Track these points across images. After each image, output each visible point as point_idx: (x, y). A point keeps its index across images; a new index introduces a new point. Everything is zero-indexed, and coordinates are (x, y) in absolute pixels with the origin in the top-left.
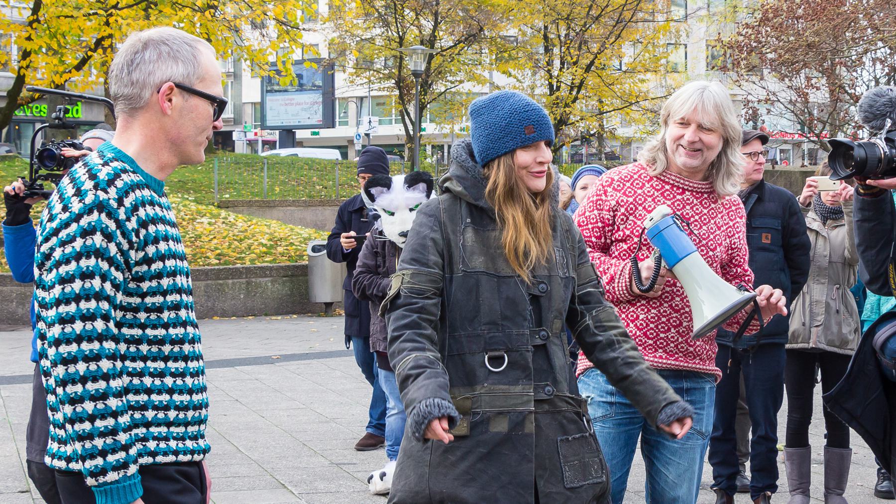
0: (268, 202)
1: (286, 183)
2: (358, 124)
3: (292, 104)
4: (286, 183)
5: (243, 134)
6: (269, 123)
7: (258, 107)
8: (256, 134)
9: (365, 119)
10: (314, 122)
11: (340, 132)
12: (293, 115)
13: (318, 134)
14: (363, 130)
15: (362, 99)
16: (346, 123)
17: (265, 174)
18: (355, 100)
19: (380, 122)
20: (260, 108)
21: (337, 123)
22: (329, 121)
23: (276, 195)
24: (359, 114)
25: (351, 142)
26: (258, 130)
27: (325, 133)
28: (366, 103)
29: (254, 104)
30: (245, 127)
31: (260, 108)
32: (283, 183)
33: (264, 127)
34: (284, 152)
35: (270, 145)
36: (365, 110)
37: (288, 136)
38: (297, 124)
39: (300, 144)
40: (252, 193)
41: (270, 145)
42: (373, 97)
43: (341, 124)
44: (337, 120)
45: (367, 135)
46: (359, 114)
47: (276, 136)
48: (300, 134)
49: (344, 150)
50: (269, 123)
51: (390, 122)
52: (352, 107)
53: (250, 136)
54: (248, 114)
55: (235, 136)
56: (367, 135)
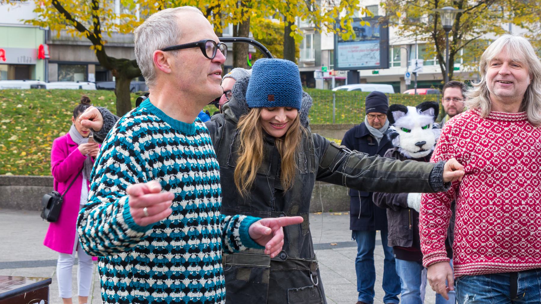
0: (336, 126)
1: (351, 111)
2: (408, 64)
3: (357, 51)
4: (351, 111)
5: (320, 74)
6: (340, 65)
7: (333, 52)
8: (330, 73)
9: (413, 61)
11: (393, 71)
12: (358, 59)
13: (377, 73)
14: (411, 69)
15: (410, 46)
16: (399, 65)
17: (334, 104)
18: (405, 47)
19: (425, 64)
20: (334, 53)
21: (392, 65)
22: (385, 63)
23: (342, 120)
24: (409, 57)
25: (402, 78)
26: (332, 71)
27: (383, 72)
28: (413, 48)
29: (330, 51)
30: (323, 69)
31: (334, 53)
32: (349, 111)
33: (336, 68)
34: (350, 87)
35: (340, 82)
36: (413, 54)
37: (354, 75)
38: (361, 66)
39: (364, 81)
40: (325, 120)
41: (340, 82)
42: (420, 45)
43: (395, 65)
44: (392, 62)
45: (415, 74)
46: (409, 57)
47: (344, 75)
48: (363, 73)
49: (396, 85)
50: (340, 65)
51: (432, 63)
53: (327, 75)
54: (326, 58)
55: (316, 75)
56: (415, 74)
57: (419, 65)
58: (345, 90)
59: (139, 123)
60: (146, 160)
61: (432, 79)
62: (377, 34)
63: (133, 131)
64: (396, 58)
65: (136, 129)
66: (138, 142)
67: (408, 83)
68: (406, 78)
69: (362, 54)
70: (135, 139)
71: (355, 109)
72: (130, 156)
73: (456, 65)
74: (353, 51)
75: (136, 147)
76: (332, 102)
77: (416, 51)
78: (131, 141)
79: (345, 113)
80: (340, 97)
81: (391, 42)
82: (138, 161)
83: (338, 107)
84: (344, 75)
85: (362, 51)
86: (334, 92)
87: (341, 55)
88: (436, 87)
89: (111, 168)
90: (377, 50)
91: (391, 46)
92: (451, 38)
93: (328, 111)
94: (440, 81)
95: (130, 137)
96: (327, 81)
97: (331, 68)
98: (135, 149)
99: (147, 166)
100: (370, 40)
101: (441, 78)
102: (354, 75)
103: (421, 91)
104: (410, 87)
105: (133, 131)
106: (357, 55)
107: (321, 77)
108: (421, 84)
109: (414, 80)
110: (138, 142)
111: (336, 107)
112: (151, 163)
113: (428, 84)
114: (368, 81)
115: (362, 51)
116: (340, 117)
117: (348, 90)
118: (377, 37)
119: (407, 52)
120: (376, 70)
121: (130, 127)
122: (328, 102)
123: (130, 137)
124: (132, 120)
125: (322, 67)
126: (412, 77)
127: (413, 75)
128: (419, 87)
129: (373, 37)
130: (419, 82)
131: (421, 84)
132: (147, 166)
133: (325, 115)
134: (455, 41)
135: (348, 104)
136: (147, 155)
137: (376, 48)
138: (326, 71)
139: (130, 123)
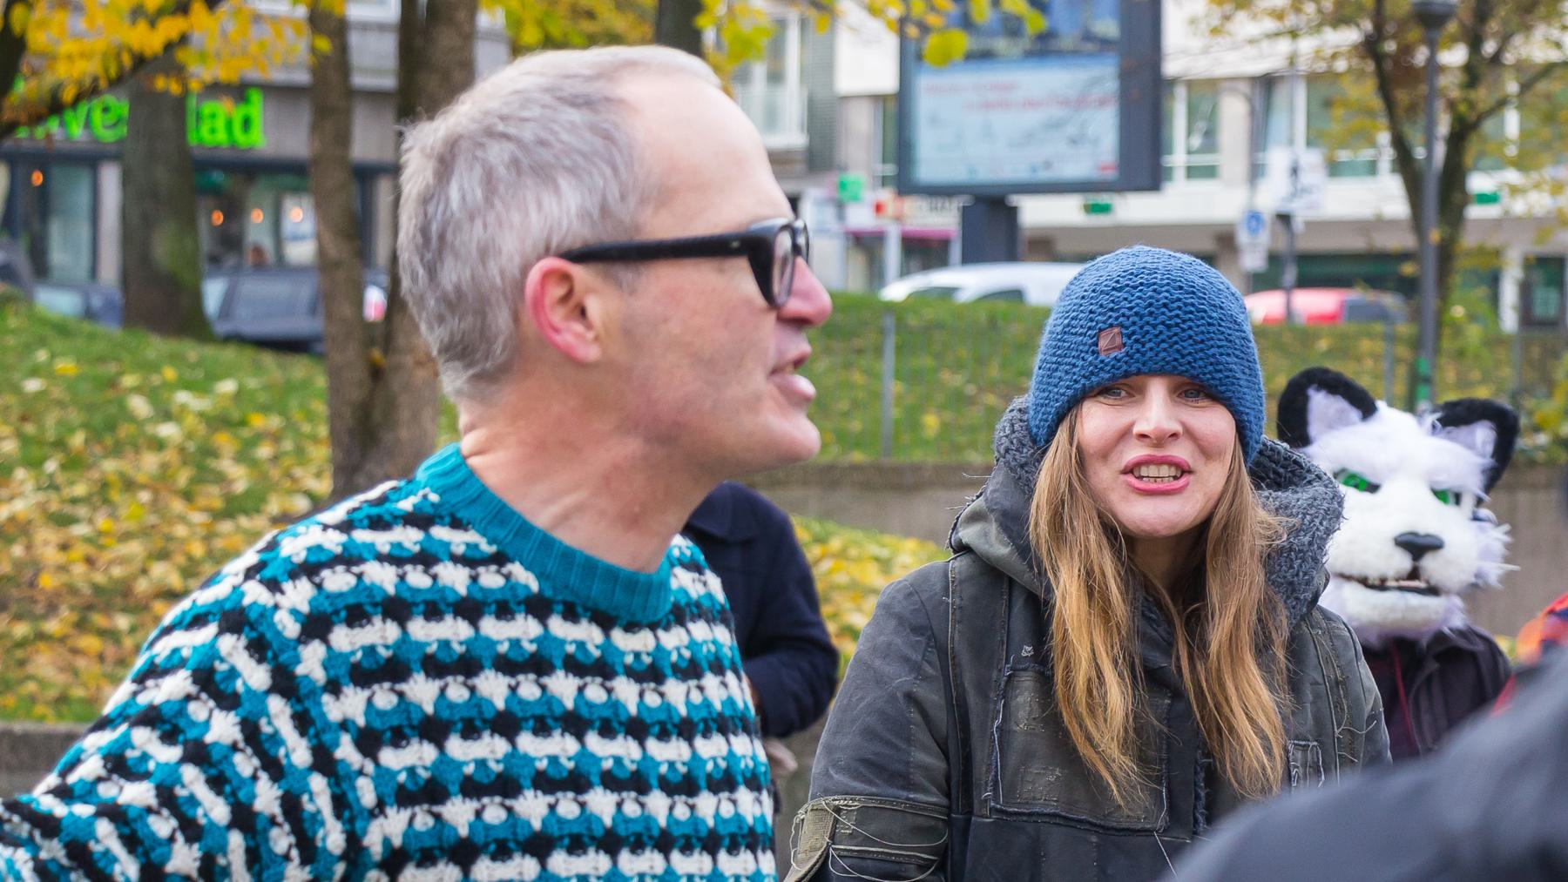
1: (971, 401)
2: (1256, 172)
3: (1005, 105)
4: (971, 401)
7: (892, 107)
9: (1277, 160)
10: (1077, 167)
11: (1181, 202)
13: (1105, 209)
14: (1271, 195)
15: (1267, 84)
16: (1209, 172)
17: (889, 362)
18: (1244, 87)
19: (1334, 169)
20: (897, 112)
21: (1179, 174)
22: (1143, 165)
23: (925, 443)
24: (1258, 137)
27: (1135, 208)
28: (1280, 96)
29: (878, 99)
30: (842, 186)
31: (897, 112)
33: (905, 184)
34: (971, 281)
35: (924, 251)
36: (1279, 121)
37: (991, 223)
39: (1045, 247)
40: (846, 440)
41: (924, 251)
42: (1313, 79)
43: (1192, 172)
44: (1178, 158)
45: (1284, 219)
46: (1258, 137)
47: (943, 219)
48: (1035, 212)
50: (928, 169)
51: (1372, 168)
52: (1234, 112)
56: (1284, 219)
57: (1306, 178)
58: (948, 293)
59: (360, 560)
60: (344, 725)
61: (1356, 243)
62: (1108, 27)
63: (319, 586)
64: (1196, 141)
65: (338, 581)
66: (325, 641)
67: (1253, 260)
68: (1243, 237)
69: (1032, 118)
70: (316, 626)
71: (991, 387)
72: (269, 691)
73: (1478, 182)
74: (988, 106)
75: (311, 662)
76: (879, 351)
77: (1295, 104)
78: (292, 629)
79: (941, 408)
80: (927, 332)
81: (1171, 68)
82: (303, 722)
83: (910, 377)
84: (943, 219)
85: (1031, 104)
86: (891, 308)
87: (935, 121)
88: (1375, 282)
89: (216, 756)
90: (1102, 103)
91: (1173, 82)
92: (1455, 56)
93: (860, 395)
94: (1405, 256)
95: (294, 612)
96: (866, 244)
97: (884, 181)
98: (300, 670)
99: (346, 751)
100: (1075, 53)
101: (1403, 240)
102: (991, 223)
103: (1315, 302)
104: (1262, 282)
105: (319, 586)
106: (1009, 123)
107: (834, 226)
108: (1318, 270)
109: (1282, 245)
110: (325, 641)
111: (898, 376)
112: (368, 742)
113: (1345, 269)
114: (1062, 247)
115: (1031, 104)
116: (914, 425)
117: (964, 297)
118: (1105, 44)
119: (1252, 113)
120: (1104, 198)
121: (309, 569)
122: (860, 352)
123: (294, 612)
124: (334, 541)
125: (834, 178)
126: (1274, 235)
127: (1280, 227)
128: (1305, 282)
129: (1088, 37)
130: (1304, 259)
131: (1317, 269)
132: (346, 751)
133: (846, 415)
134: (1472, 74)
135: (958, 366)
136: (351, 705)
137: (1097, 92)
138: (856, 199)
139: (319, 548)
